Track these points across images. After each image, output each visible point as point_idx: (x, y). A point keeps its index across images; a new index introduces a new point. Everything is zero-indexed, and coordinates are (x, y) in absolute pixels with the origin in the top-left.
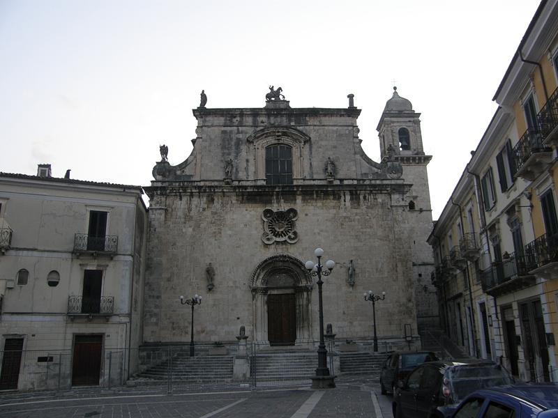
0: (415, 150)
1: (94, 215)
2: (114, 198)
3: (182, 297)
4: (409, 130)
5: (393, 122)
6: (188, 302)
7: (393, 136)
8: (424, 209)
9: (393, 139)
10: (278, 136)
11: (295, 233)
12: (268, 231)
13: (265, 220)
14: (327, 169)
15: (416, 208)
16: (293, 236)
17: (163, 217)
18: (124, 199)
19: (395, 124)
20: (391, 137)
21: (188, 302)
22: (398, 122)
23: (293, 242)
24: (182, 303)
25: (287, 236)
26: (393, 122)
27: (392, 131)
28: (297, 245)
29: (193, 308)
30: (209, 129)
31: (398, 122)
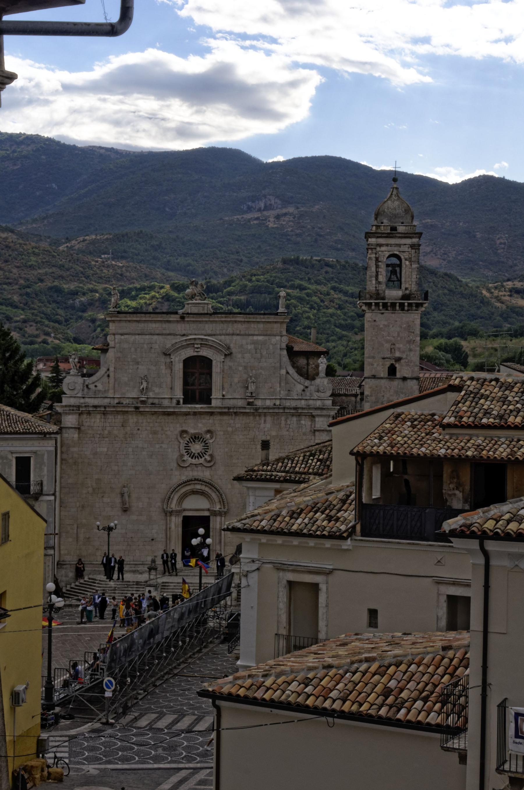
0: (406, 289)
1: (19, 460)
2: (36, 443)
3: (98, 523)
4: (402, 257)
5: (381, 245)
6: (104, 529)
7: (377, 266)
8: (400, 380)
9: (377, 272)
10: (197, 348)
11: (211, 456)
12: (184, 452)
13: (182, 441)
14: (247, 388)
15: (398, 375)
16: (208, 458)
17: (76, 436)
18: (45, 442)
19: (383, 249)
20: (373, 269)
21: (104, 529)
22: (387, 245)
23: (212, 464)
24: (98, 529)
25: (203, 458)
26: (381, 245)
27: (377, 259)
28: (213, 468)
29: (109, 534)
30: (123, 337)
31: (387, 245)
